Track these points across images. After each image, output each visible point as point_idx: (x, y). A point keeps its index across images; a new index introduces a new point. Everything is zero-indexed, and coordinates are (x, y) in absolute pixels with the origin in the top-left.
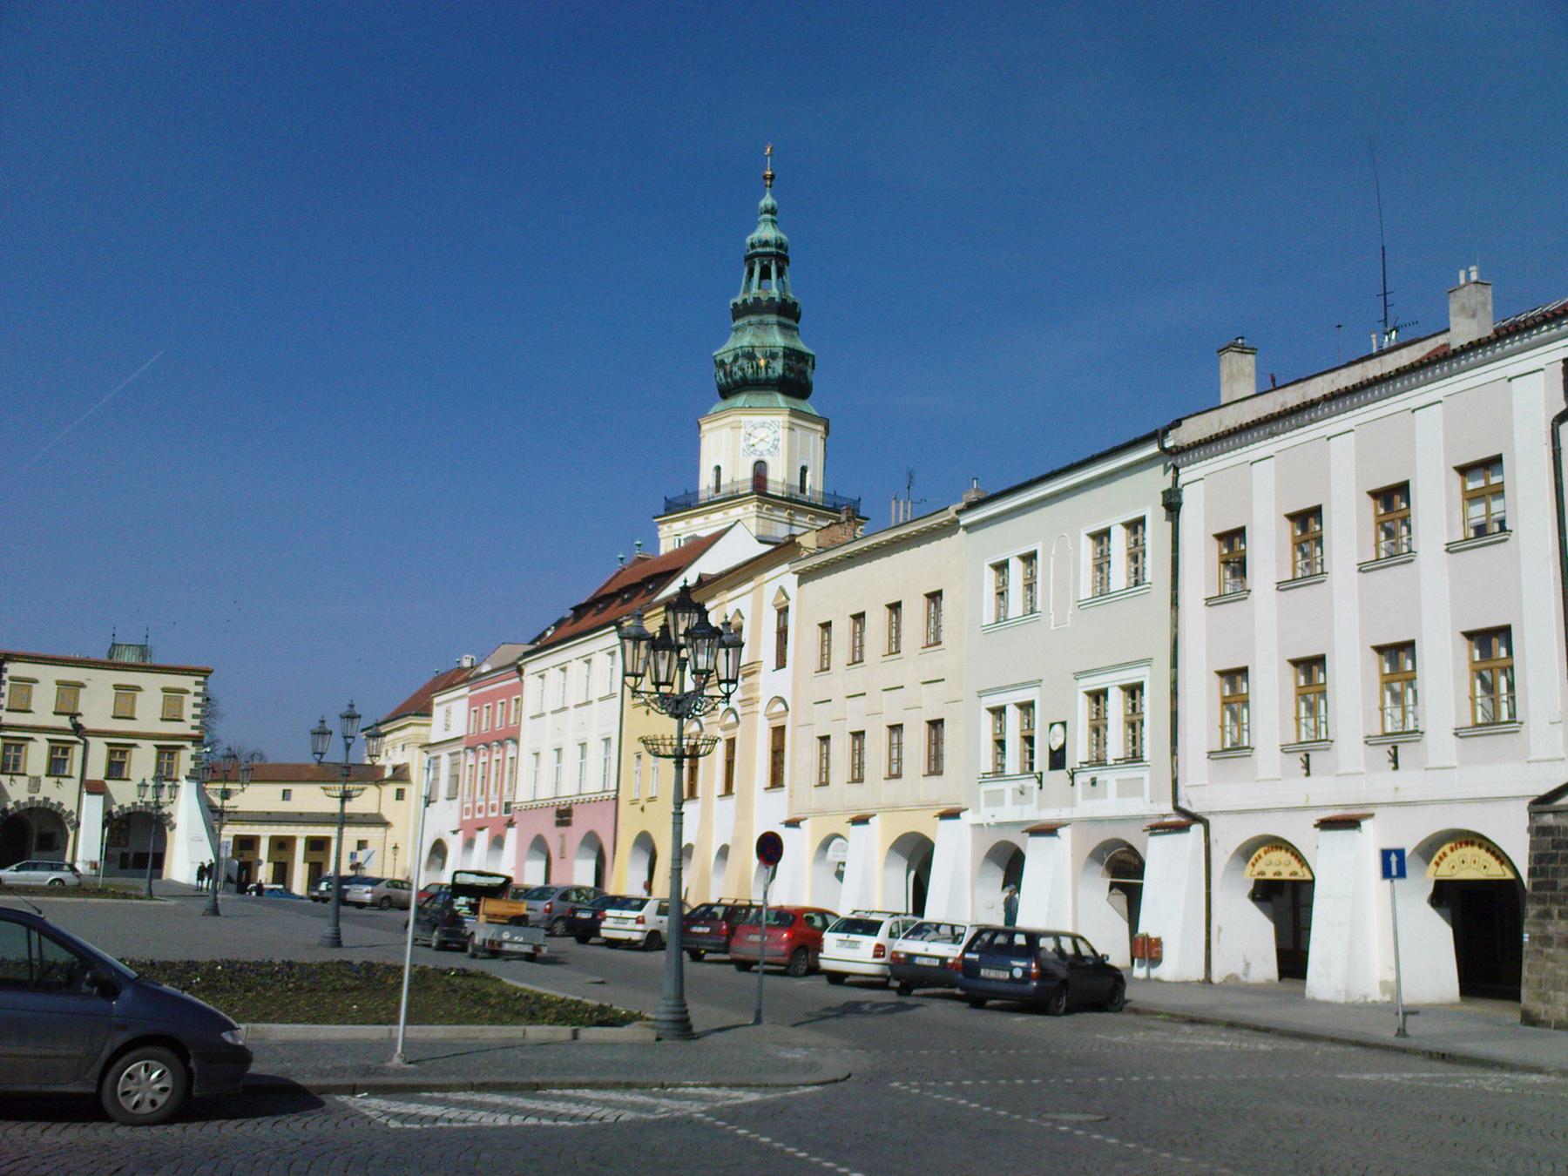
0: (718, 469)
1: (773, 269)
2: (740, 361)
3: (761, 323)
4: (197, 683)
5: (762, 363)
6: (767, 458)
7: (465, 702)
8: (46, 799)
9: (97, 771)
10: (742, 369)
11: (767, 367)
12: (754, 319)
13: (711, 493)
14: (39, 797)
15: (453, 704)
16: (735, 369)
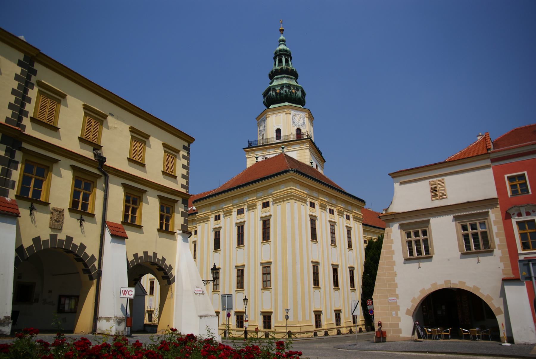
0: (278, 131)
1: (289, 60)
2: (285, 89)
3: (289, 78)
4: (184, 148)
5: (294, 91)
6: (301, 128)
7: (490, 171)
8: (69, 239)
9: (116, 214)
10: (286, 91)
11: (296, 93)
12: (286, 75)
13: (275, 139)
14: (62, 236)
15: (447, 179)
16: (282, 92)
